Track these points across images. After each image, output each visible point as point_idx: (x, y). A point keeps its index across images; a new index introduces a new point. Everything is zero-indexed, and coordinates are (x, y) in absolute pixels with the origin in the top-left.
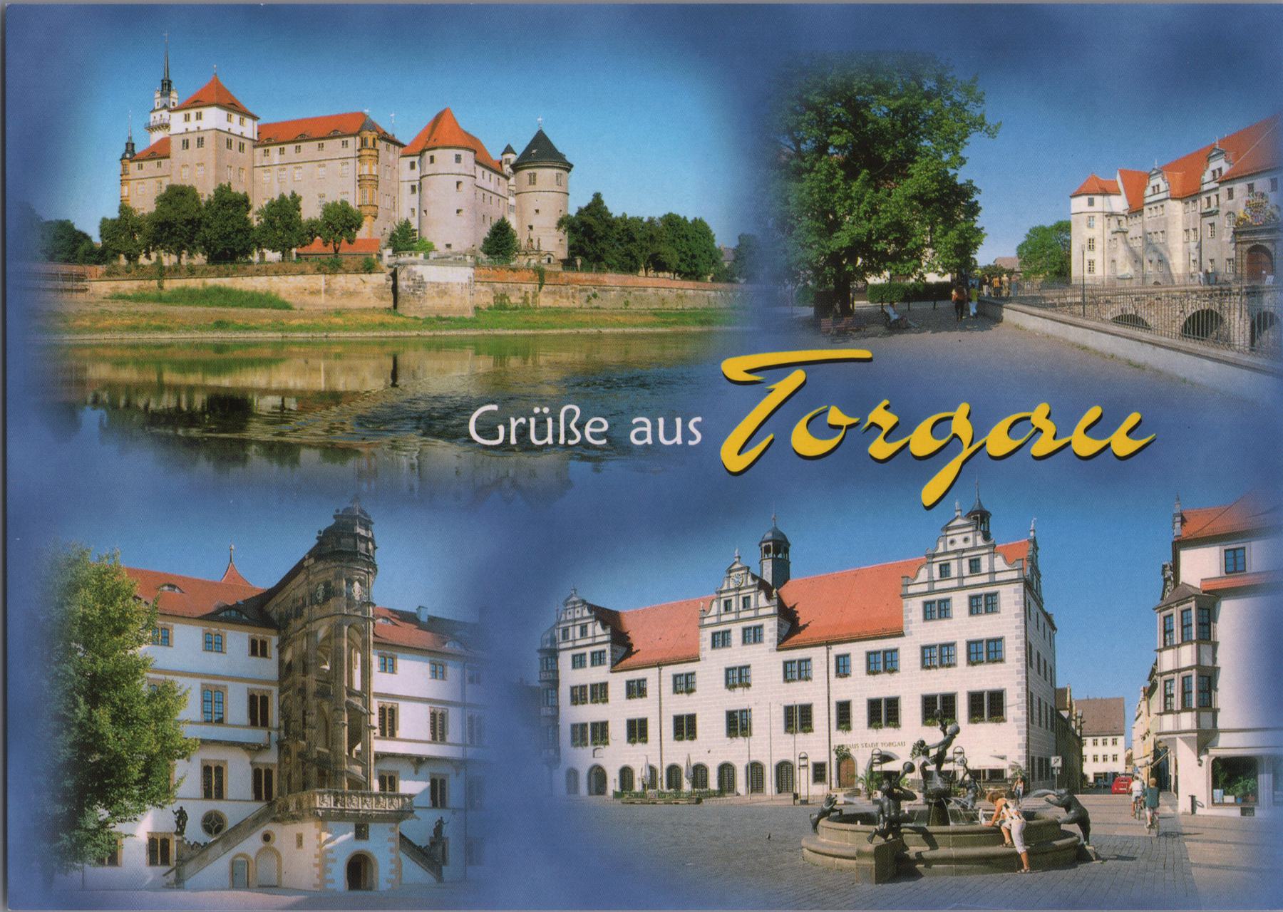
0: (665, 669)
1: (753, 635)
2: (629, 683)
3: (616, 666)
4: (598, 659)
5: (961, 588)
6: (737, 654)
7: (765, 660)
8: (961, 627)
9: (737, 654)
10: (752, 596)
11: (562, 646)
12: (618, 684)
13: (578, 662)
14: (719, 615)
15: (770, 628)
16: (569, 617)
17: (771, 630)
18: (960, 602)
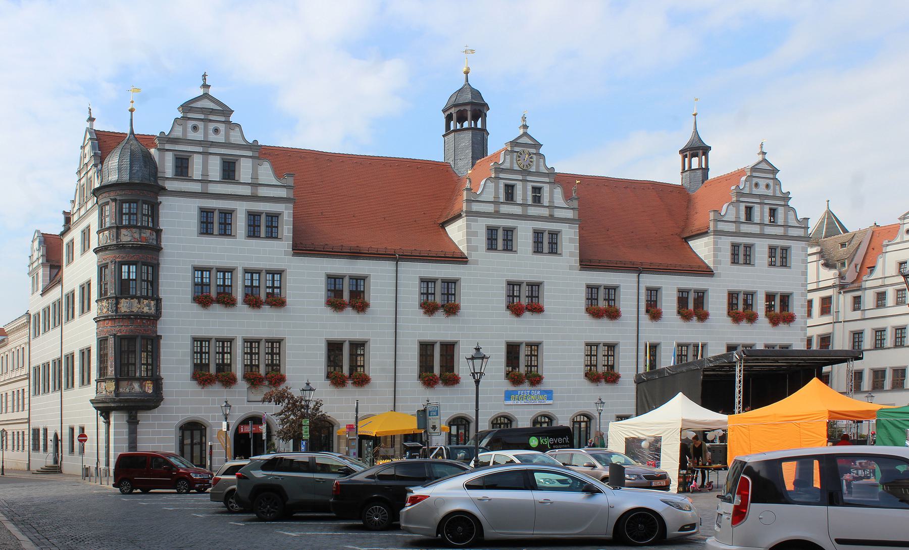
0: (405, 266)
1: (546, 243)
2: (333, 280)
3: (301, 248)
4: (262, 226)
5: (762, 235)
6: (524, 264)
7: (564, 280)
8: (760, 279)
9: (524, 264)
10: (546, 189)
11: (170, 186)
12: (307, 278)
13: (214, 223)
14: (496, 203)
15: (569, 238)
16: (199, 136)
17: (571, 240)
18: (761, 249)
